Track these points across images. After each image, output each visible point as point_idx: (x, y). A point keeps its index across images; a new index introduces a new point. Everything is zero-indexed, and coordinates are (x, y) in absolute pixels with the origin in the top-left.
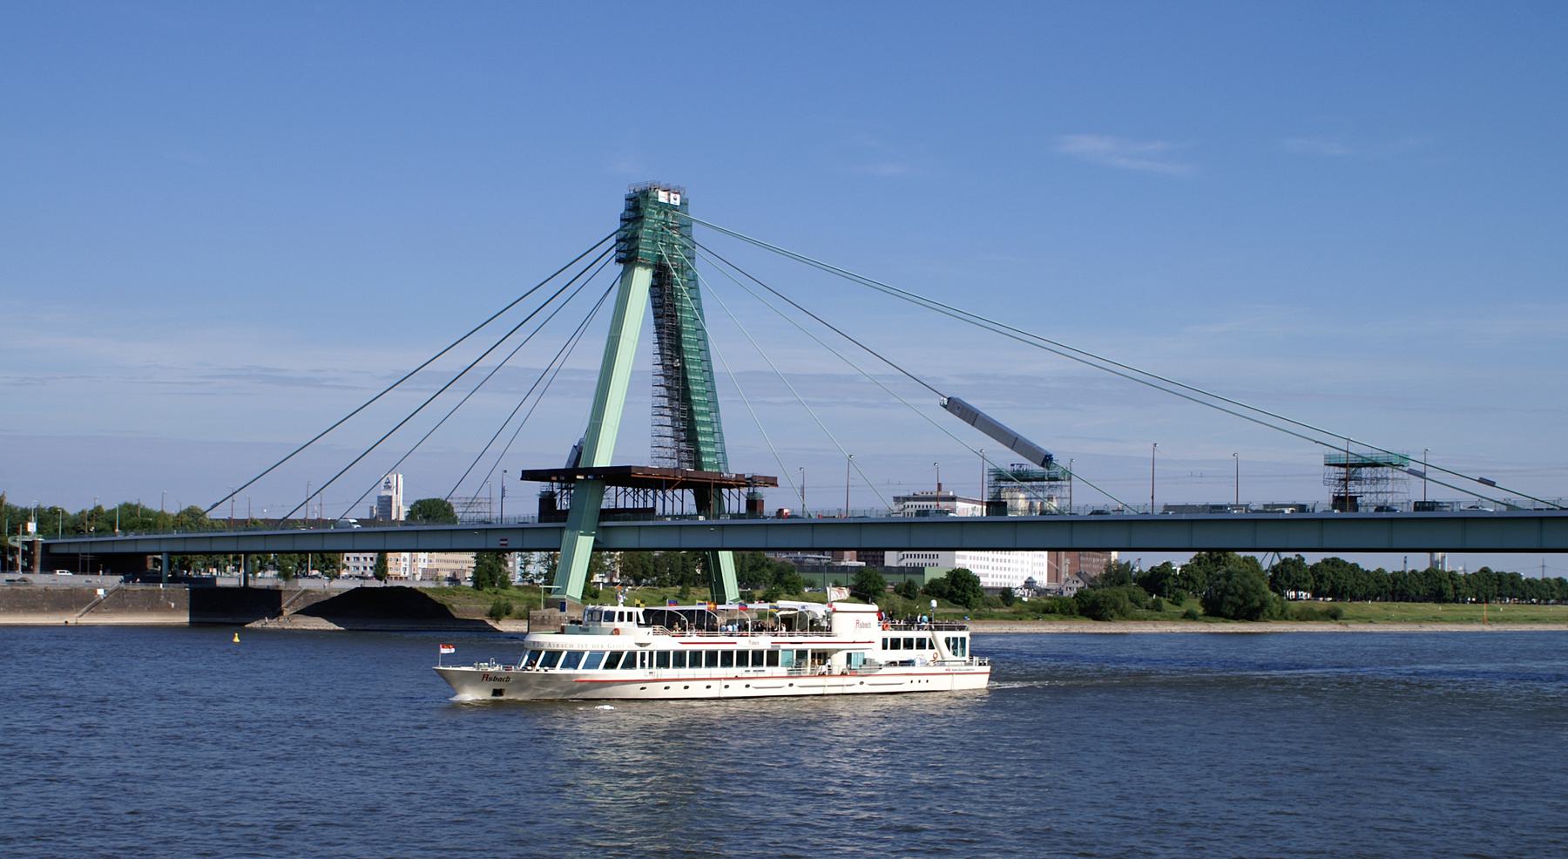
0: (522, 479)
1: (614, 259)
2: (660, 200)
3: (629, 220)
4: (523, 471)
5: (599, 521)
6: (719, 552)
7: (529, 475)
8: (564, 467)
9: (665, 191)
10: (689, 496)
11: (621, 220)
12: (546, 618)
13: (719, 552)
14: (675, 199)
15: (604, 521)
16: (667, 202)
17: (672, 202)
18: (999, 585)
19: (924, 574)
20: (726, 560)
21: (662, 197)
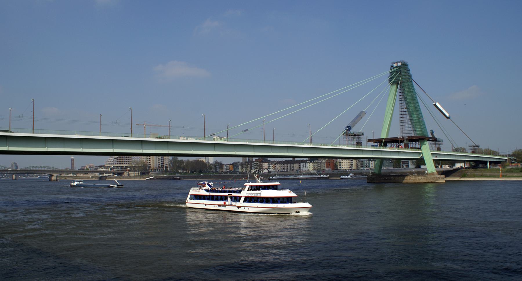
16: (396, 66)
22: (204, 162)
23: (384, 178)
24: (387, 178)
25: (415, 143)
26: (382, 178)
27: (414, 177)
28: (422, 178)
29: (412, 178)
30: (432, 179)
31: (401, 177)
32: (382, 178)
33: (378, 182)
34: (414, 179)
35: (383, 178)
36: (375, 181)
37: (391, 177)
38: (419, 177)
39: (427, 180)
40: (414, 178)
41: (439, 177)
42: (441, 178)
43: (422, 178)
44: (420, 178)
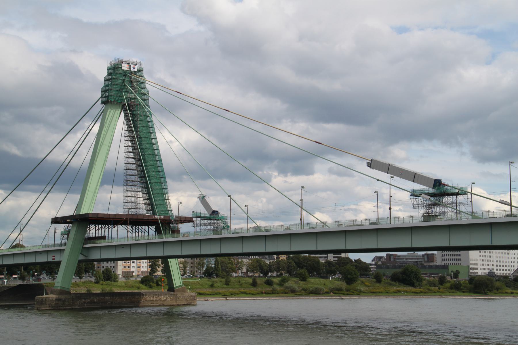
0: (52, 223)
1: (100, 101)
2: (123, 68)
3: (108, 80)
4: (52, 219)
5: (84, 244)
6: (169, 259)
7: (56, 221)
8: (72, 214)
9: (128, 64)
10: (152, 229)
11: (105, 80)
13: (169, 259)
14: (134, 68)
15: (87, 244)
16: (128, 69)
17: (132, 69)
18: (502, 275)
19: (448, 269)
20: (174, 265)
21: (125, 67)
23: (90, 300)
24: (95, 300)
25: (140, 228)
26: (85, 299)
28: (167, 298)
29: (148, 299)
31: (128, 297)
32: (85, 299)
34: (153, 300)
35: (87, 300)
38: (163, 296)
39: (176, 300)
40: (152, 299)
41: (195, 295)
43: (167, 298)
44: (165, 298)
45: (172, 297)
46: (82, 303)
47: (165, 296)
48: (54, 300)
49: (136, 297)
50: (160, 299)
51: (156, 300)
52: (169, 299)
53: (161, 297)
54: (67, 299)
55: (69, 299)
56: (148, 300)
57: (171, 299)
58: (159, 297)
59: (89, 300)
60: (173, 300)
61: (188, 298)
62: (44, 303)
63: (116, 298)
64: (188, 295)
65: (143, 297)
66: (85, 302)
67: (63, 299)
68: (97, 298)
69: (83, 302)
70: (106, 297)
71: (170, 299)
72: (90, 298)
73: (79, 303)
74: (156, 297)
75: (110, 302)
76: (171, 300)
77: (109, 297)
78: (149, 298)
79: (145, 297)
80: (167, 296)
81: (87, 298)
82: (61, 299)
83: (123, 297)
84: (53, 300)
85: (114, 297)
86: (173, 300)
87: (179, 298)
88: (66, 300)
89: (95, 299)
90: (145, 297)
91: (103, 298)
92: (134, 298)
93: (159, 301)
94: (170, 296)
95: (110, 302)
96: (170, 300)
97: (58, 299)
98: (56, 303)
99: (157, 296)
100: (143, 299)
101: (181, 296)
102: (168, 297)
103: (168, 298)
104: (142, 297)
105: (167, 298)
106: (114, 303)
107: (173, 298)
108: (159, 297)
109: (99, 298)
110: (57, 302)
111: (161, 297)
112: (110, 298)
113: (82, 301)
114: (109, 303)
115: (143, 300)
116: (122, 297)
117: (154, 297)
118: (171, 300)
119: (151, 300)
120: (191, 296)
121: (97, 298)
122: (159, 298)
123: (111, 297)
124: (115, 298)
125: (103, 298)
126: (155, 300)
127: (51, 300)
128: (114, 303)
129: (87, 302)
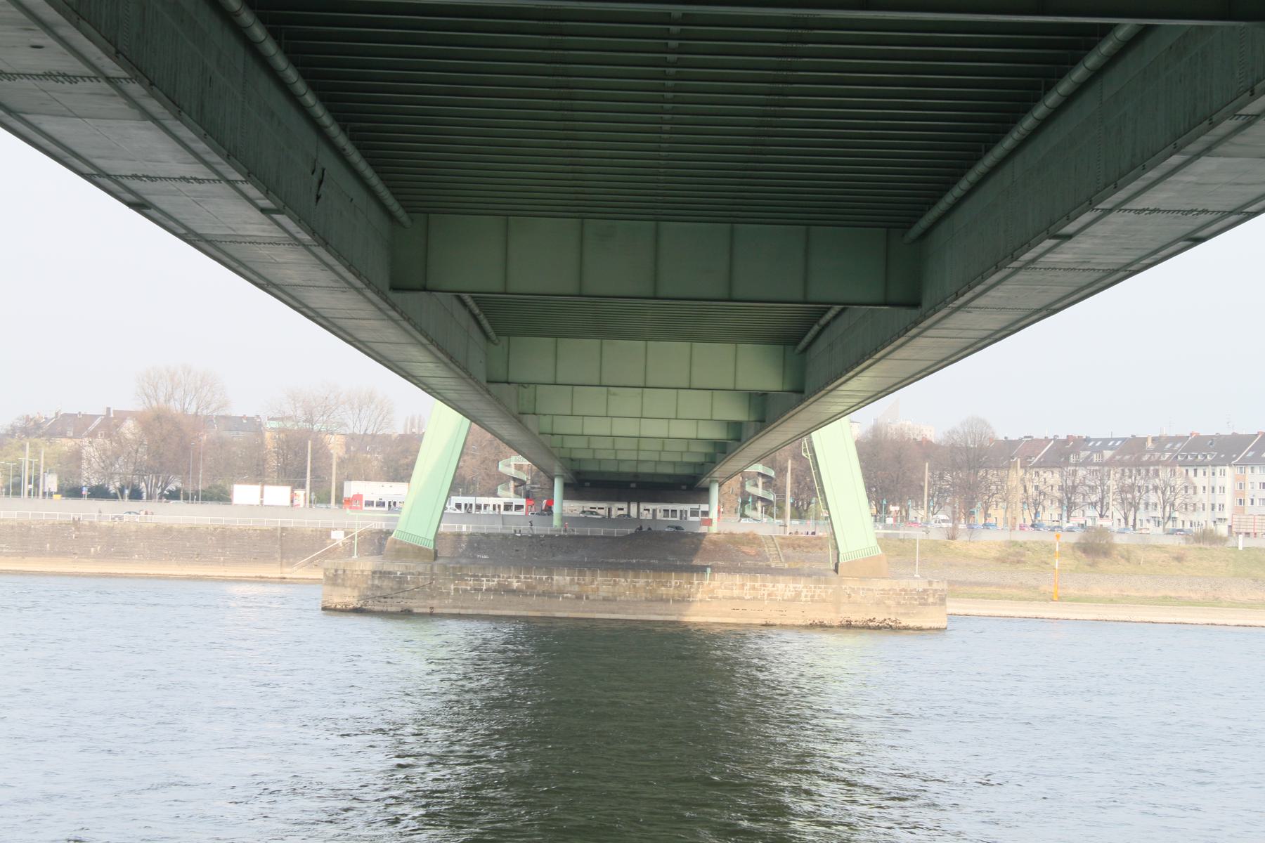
12: (340, 572)
22: (931, 442)
23: (494, 583)
24: (515, 585)
27: (738, 579)
28: (798, 594)
30: (879, 603)
31: (641, 582)
33: (437, 611)
35: (485, 584)
36: (417, 605)
37: (555, 577)
38: (780, 586)
40: (736, 592)
41: (925, 591)
42: (931, 600)
43: (798, 594)
44: (788, 594)
45: (818, 591)
46: (465, 591)
47: (791, 586)
48: (368, 575)
49: (673, 583)
50: (769, 595)
51: (755, 599)
52: (806, 596)
53: (774, 586)
54: (413, 574)
55: (420, 574)
56: (720, 596)
57: (816, 598)
58: (765, 586)
59: (491, 583)
60: (824, 601)
61: (889, 598)
62: (340, 581)
63: (596, 583)
64: (887, 588)
65: (699, 584)
66: (478, 590)
67: (399, 573)
68: (522, 576)
69: (469, 588)
70: (555, 577)
71: (812, 596)
72: (494, 576)
73: (456, 590)
74: (753, 588)
75: (569, 595)
76: (817, 601)
77: (568, 578)
78: (726, 588)
79: (710, 584)
80: (801, 586)
81: (482, 576)
82: (390, 573)
83: (623, 580)
84: (365, 573)
85: (587, 578)
86: (824, 601)
87: (849, 596)
88: (409, 577)
89: (515, 580)
90: (710, 584)
91: (544, 577)
92: (666, 587)
93: (766, 602)
94: (813, 586)
95: (569, 595)
96: (812, 601)
97: (380, 572)
98: (373, 585)
99: (757, 585)
100: (700, 590)
101: (859, 589)
102: (805, 590)
103: (803, 594)
104: (696, 582)
105: (802, 591)
106: (587, 598)
107: (823, 594)
108: (765, 586)
109: (531, 578)
110: (376, 582)
111: (774, 586)
112: (572, 580)
113: (466, 585)
114: (567, 598)
115: (699, 596)
116: (617, 579)
117: (743, 585)
118: (817, 601)
119: (732, 598)
120: (905, 590)
121: (522, 576)
122: (766, 593)
123: (576, 578)
124: (592, 583)
125: (544, 577)
126: (748, 597)
127: (359, 573)
128: (587, 598)
129: (484, 588)
